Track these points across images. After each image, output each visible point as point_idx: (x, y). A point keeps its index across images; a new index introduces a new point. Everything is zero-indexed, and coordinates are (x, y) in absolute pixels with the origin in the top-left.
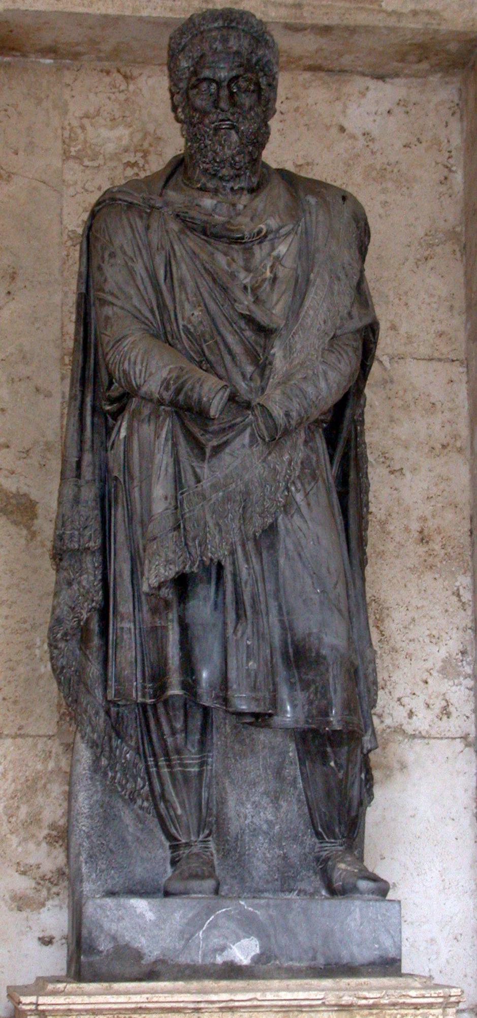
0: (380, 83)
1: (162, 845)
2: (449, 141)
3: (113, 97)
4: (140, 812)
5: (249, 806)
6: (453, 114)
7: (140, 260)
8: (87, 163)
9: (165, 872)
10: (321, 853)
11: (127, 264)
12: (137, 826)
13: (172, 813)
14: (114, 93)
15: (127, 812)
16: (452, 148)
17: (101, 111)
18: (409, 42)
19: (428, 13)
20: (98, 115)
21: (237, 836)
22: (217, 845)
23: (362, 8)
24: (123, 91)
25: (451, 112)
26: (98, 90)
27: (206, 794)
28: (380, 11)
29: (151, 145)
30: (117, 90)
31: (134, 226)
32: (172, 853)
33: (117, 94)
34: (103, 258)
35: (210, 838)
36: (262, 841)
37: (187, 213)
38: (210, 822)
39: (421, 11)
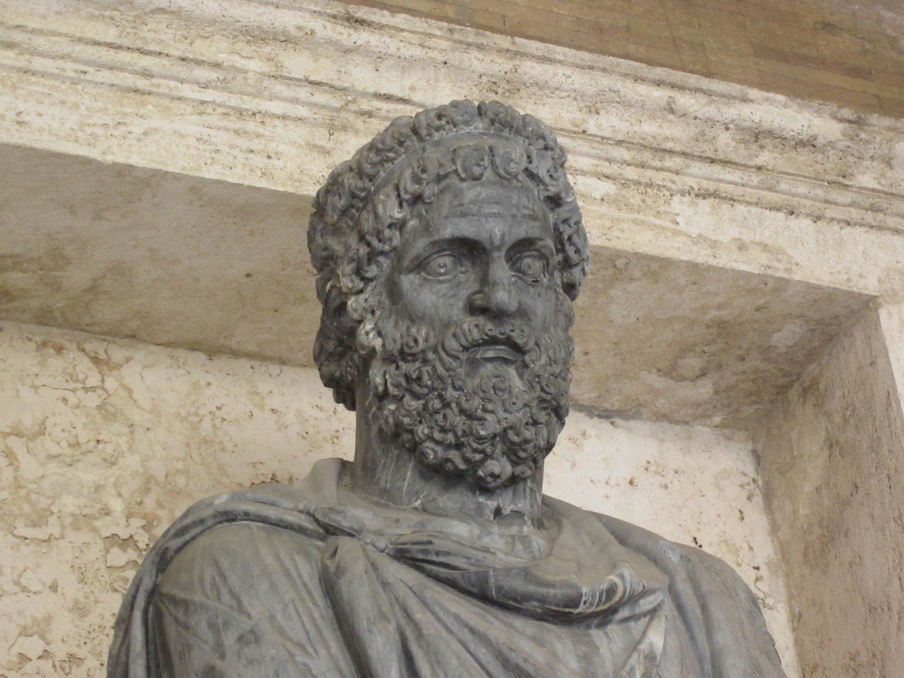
0: (605, 425)
2: (751, 548)
3: (72, 399)
6: (749, 498)
7: (322, 652)
8: (22, 530)
11: (292, 656)
14: (74, 391)
16: (760, 561)
17: (49, 424)
18: (713, 313)
19: (765, 247)
20: (42, 432)
23: (643, 221)
24: (93, 389)
25: (745, 494)
26: (38, 382)
28: (676, 233)
29: (160, 505)
30: (79, 386)
31: (295, 574)
33: (81, 393)
34: (220, 650)
37: (430, 543)
39: (752, 242)
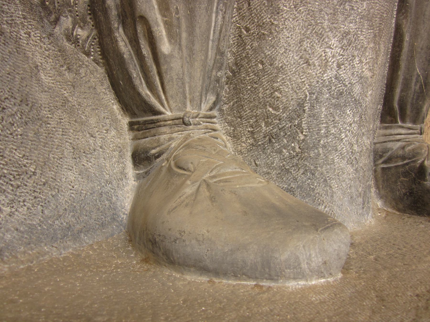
1: (115, 121)
4: (67, 45)
5: (334, 42)
9: (123, 174)
10: (389, 145)
12: (61, 74)
13: (146, 51)
15: (36, 35)
21: (301, 105)
22: (230, 124)
27: (220, 18)
32: (135, 138)
35: (215, 112)
36: (349, 120)
38: (218, 80)
